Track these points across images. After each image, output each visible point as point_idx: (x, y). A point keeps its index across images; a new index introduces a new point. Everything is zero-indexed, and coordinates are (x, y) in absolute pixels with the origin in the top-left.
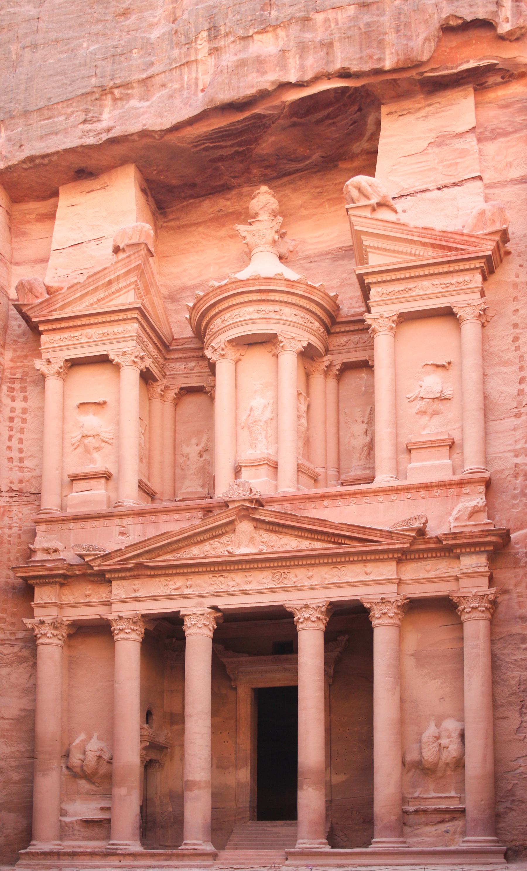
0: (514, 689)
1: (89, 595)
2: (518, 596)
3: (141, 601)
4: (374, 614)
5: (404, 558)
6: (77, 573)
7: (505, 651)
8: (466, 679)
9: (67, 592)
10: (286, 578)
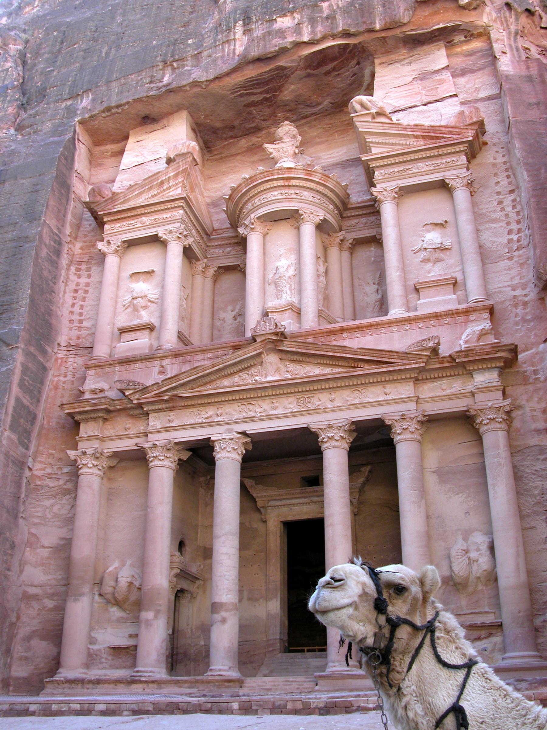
0: (538, 498)
1: (129, 429)
2: (531, 411)
3: (176, 430)
5: (420, 378)
6: (118, 407)
7: (525, 463)
8: (490, 488)
9: (109, 427)
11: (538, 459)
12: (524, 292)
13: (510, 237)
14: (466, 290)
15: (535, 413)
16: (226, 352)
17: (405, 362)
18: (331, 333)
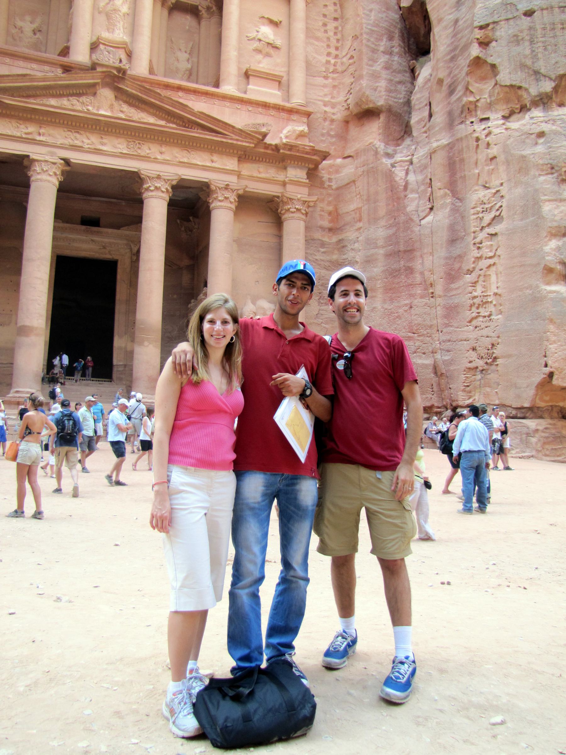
4: (217, 197)
10: (139, 148)
11: (319, 251)
12: (332, 111)
13: (329, 59)
14: (288, 92)
15: (323, 213)
16: (53, 69)
17: (237, 138)
18: (167, 86)
